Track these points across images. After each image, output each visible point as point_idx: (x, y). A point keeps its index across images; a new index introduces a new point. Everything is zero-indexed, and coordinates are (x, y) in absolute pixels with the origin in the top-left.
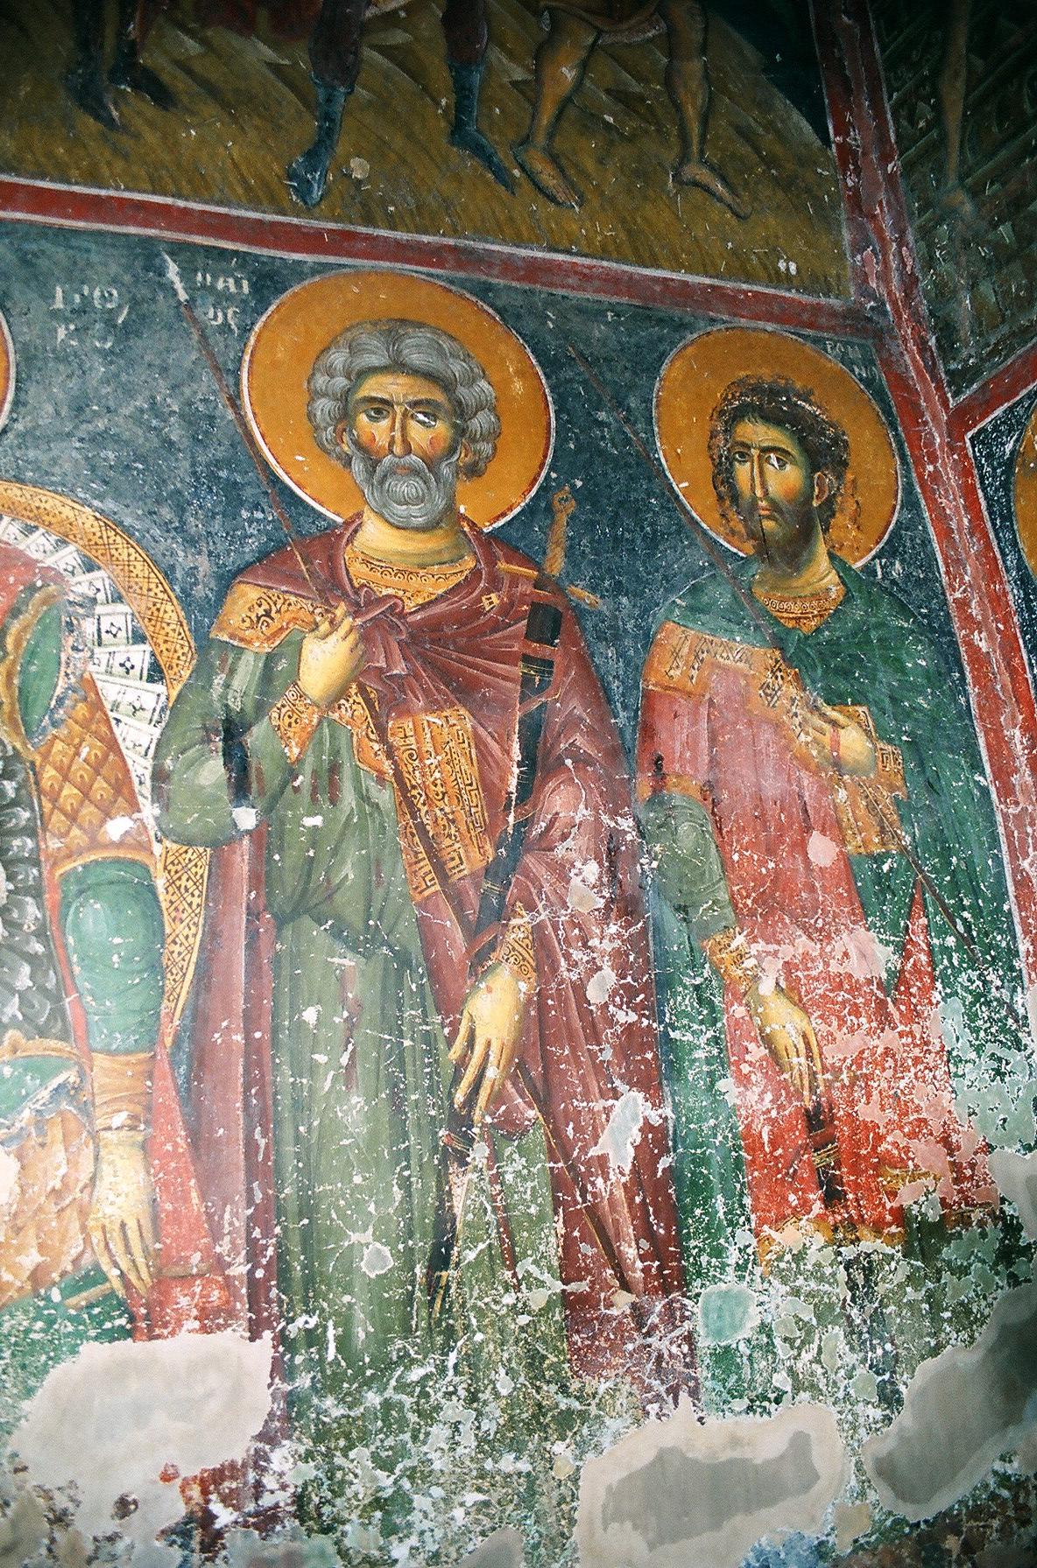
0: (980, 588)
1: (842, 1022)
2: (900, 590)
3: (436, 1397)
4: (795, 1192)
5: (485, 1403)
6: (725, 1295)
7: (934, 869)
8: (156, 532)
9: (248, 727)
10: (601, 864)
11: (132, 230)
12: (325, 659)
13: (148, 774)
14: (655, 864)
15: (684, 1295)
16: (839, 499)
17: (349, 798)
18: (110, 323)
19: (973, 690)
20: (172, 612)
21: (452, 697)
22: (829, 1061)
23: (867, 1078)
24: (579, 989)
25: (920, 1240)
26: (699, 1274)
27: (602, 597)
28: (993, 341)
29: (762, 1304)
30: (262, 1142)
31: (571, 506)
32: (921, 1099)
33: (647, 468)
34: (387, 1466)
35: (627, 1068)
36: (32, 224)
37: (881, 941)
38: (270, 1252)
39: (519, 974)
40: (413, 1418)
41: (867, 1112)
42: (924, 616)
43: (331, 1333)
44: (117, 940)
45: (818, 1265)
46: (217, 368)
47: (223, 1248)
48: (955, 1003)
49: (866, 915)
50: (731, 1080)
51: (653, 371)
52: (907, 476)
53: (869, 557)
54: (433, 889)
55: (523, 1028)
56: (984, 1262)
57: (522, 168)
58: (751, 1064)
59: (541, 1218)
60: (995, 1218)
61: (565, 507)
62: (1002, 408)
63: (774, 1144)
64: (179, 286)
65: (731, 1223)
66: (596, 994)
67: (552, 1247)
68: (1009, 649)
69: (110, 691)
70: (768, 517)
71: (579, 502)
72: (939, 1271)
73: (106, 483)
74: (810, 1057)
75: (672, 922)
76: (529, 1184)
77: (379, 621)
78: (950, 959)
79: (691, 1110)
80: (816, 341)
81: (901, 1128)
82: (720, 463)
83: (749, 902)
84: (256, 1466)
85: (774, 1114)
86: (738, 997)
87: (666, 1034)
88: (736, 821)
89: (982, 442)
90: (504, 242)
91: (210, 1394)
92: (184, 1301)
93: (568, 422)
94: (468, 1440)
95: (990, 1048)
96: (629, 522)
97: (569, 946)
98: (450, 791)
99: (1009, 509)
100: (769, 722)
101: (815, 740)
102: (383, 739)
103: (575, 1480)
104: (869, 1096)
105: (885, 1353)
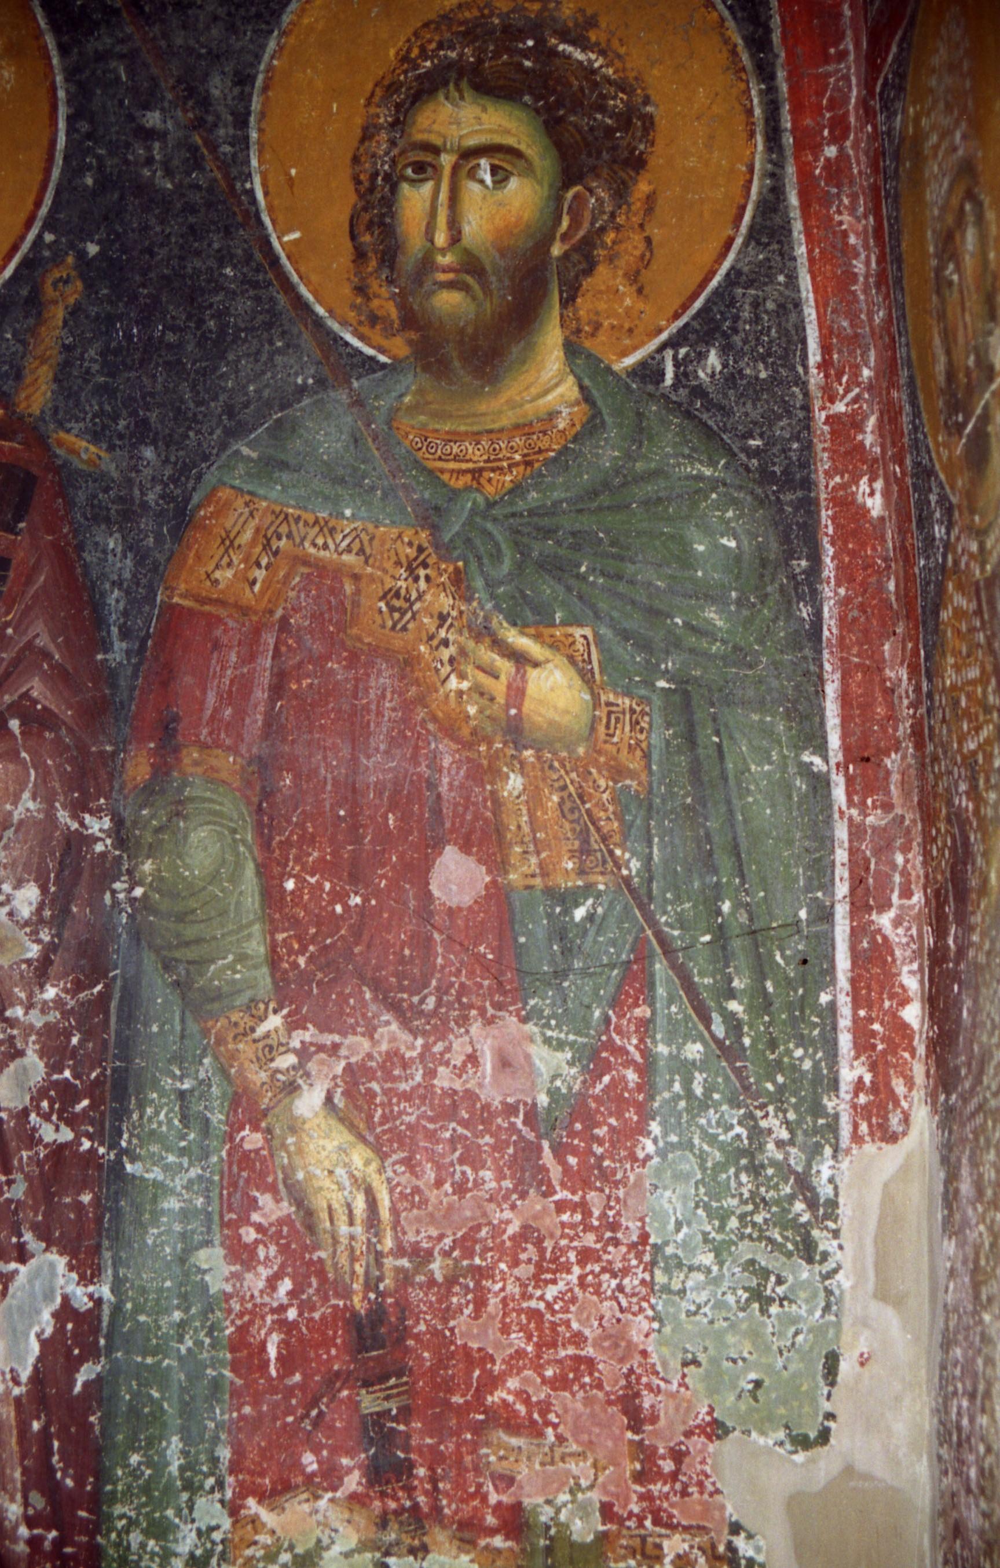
2: (710, 405)
4: (316, 1450)
7: (681, 922)
10: (44, 889)
14: (138, 892)
16: (610, 237)
22: (411, 1237)
23: (481, 1274)
27: (111, 448)
31: (75, 291)
32: (585, 1322)
33: (230, 212)
37: (547, 1041)
42: (757, 453)
49: (520, 994)
50: (219, 1252)
58: (259, 1228)
61: (64, 294)
65: (189, 1486)
70: (451, 285)
71: (90, 286)
78: (687, 1083)
81: (539, 1369)
82: (371, 190)
83: (302, 961)
87: (119, 1164)
88: (301, 825)
93: (89, 136)
95: (745, 1250)
96: (177, 313)
104: (480, 1303)
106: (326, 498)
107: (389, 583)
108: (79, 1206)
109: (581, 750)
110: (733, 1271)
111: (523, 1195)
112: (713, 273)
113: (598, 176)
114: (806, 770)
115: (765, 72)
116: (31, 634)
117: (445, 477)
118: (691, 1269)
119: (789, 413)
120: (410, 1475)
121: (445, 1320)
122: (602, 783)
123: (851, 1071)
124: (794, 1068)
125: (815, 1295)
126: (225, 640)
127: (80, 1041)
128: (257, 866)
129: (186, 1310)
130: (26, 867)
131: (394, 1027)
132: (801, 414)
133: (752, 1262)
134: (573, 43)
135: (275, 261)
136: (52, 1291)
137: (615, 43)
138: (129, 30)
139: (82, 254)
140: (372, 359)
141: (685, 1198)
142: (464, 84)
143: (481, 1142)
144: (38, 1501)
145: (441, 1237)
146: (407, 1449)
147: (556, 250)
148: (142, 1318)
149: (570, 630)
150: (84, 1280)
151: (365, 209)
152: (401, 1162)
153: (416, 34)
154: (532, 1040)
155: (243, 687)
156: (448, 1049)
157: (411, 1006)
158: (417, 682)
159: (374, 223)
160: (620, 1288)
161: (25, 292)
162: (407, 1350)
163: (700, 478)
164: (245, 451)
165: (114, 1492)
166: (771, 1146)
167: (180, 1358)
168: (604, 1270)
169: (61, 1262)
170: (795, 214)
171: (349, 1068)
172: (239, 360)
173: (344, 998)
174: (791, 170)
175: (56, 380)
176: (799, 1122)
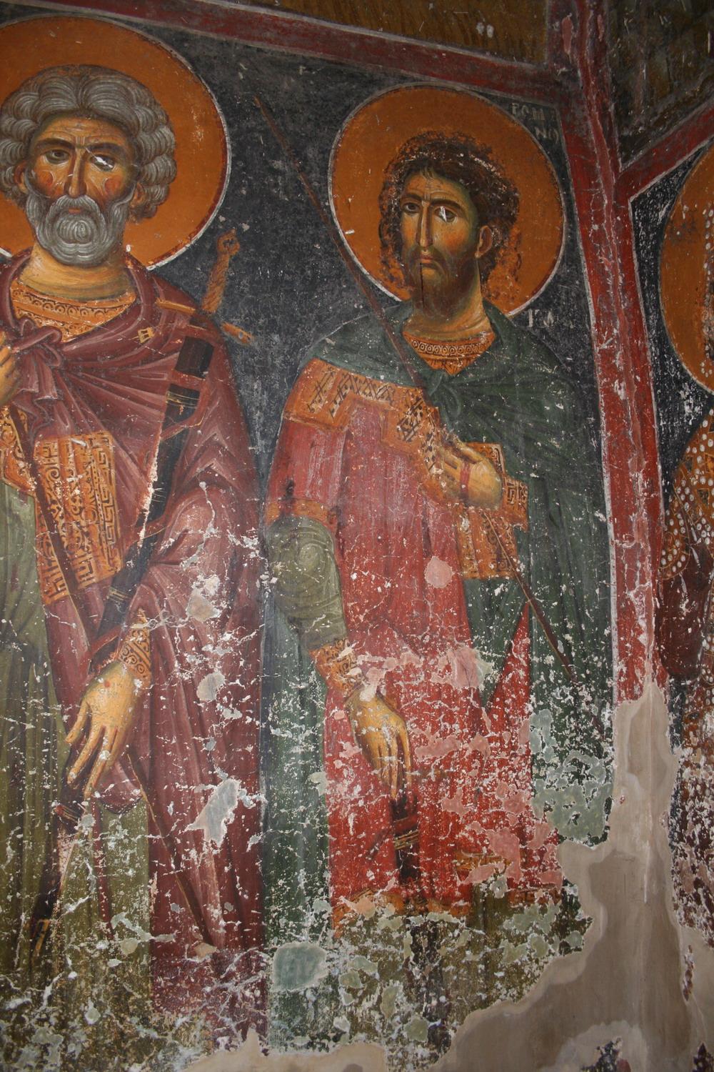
0: (625, 342)
1: (436, 726)
2: (549, 339)
4: (374, 869)
5: (73, 1030)
7: (544, 595)
10: (222, 579)
14: (274, 580)
15: (261, 950)
16: (502, 252)
19: (605, 434)
21: (98, 422)
22: (420, 760)
24: (190, 688)
25: (484, 913)
26: (277, 933)
27: (255, 334)
28: (660, 110)
29: (331, 960)
31: (236, 249)
35: (228, 758)
37: (483, 657)
39: (133, 674)
41: (446, 804)
42: (569, 364)
45: (387, 930)
48: (546, 714)
49: (472, 634)
51: (335, 123)
52: (572, 233)
53: (523, 307)
54: (63, 594)
56: (540, 932)
58: (344, 760)
59: (138, 879)
60: (556, 897)
61: (230, 250)
62: (661, 176)
63: (358, 828)
66: (204, 693)
67: (145, 904)
68: (642, 399)
70: (429, 266)
71: (244, 246)
72: (498, 939)
74: (401, 755)
75: (286, 634)
76: (129, 852)
78: (547, 676)
79: (284, 797)
80: (503, 102)
81: (480, 819)
83: (361, 617)
86: (340, 703)
87: (267, 731)
88: (359, 544)
89: (641, 208)
93: (244, 169)
95: (573, 754)
97: (184, 650)
98: (88, 506)
99: (656, 272)
100: (402, 454)
101: (446, 474)
102: (28, 457)
104: (453, 790)
105: (439, 1004)
106: (371, 369)
107: (402, 416)
108: (245, 753)
109: (496, 508)
110: (567, 764)
111: (473, 735)
112: (548, 276)
113: (495, 223)
114: (597, 519)
115: (565, 186)
116: (211, 434)
117: (429, 362)
118: (549, 765)
119: (584, 347)
120: (420, 877)
121: (436, 800)
122: (506, 524)
123: (618, 666)
124: (594, 666)
125: (602, 773)
126: (317, 442)
127: (245, 664)
128: (337, 566)
129: (306, 805)
130: (211, 565)
131: (410, 652)
132: (588, 347)
133: (575, 760)
134: (481, 158)
135: (341, 243)
136: (233, 798)
137: (500, 162)
138: (265, 119)
139: (240, 230)
140: (392, 298)
141: (546, 732)
142: (431, 169)
143: (453, 710)
144: (229, 907)
145: (434, 760)
146: (418, 864)
147: (477, 255)
148: (283, 811)
149: (490, 445)
150: (250, 792)
151: (386, 223)
152: (415, 722)
153: (408, 142)
154: (476, 657)
155: (328, 467)
156: (436, 663)
157: (418, 641)
158: (416, 469)
159: (390, 228)
160: (517, 777)
161: (208, 246)
162: (418, 816)
163: (546, 373)
164: (329, 341)
165: (270, 900)
166: (584, 704)
167: (304, 830)
168: (510, 769)
169: (237, 783)
170: (582, 253)
171: (389, 675)
172: (323, 292)
173: (385, 637)
174: (579, 233)
175: (224, 295)
176: (597, 691)
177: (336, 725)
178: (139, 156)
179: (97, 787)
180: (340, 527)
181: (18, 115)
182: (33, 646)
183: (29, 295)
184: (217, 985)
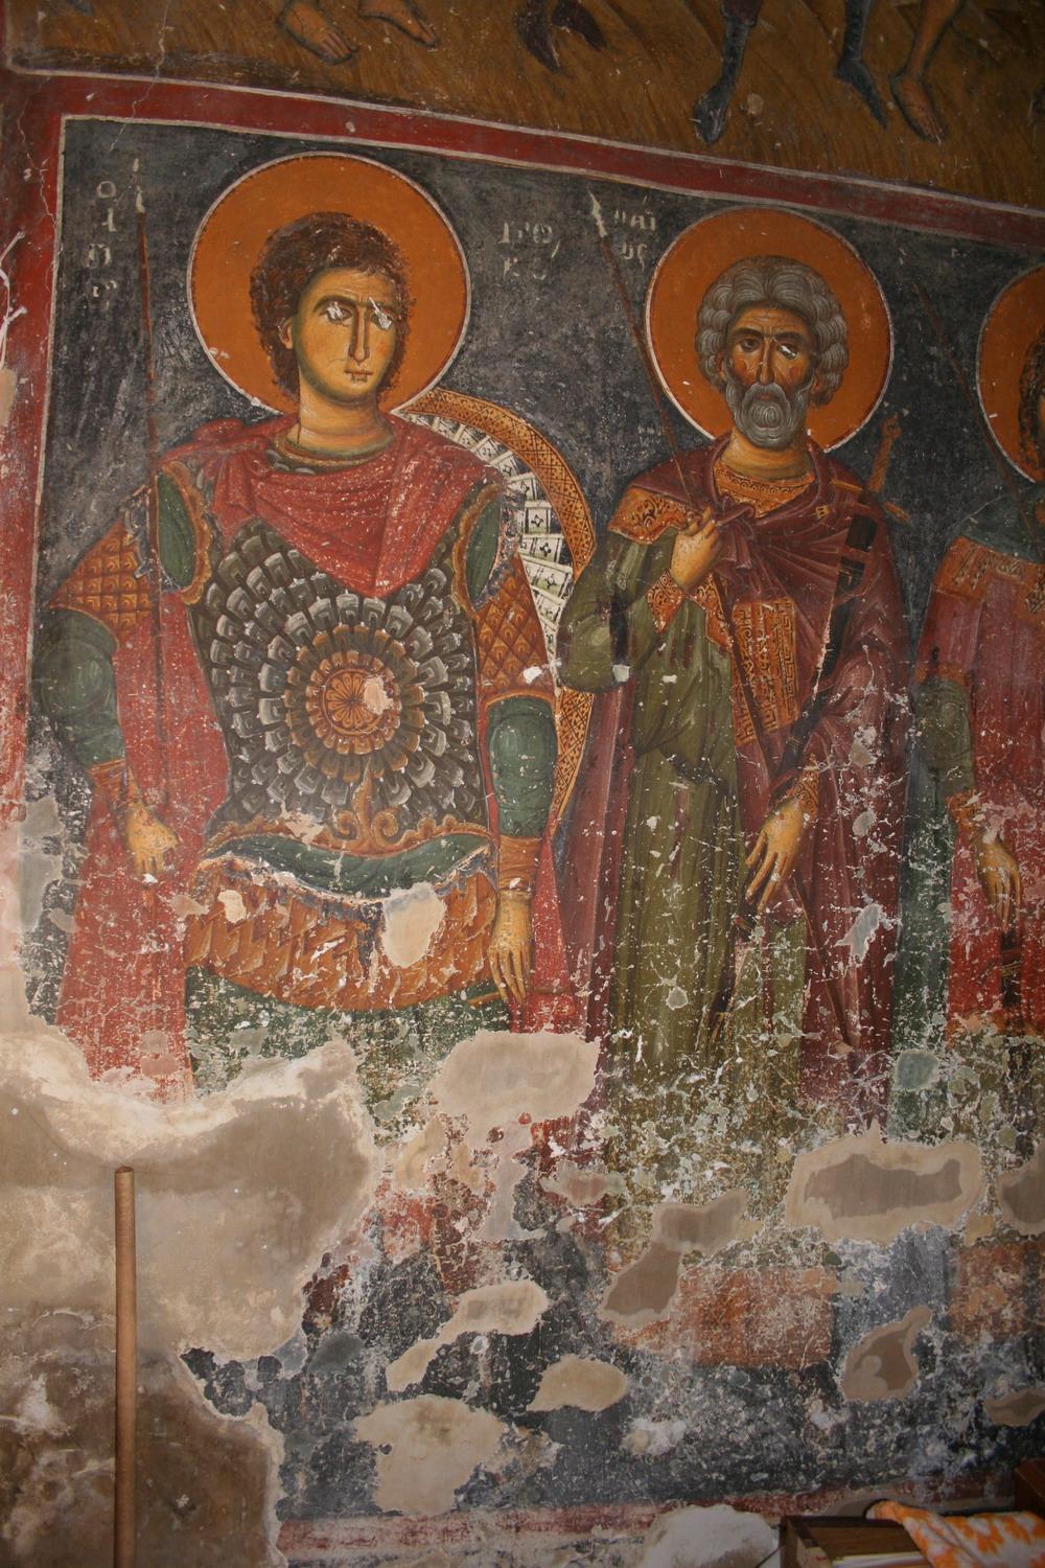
3: (705, 1096)
4: (983, 992)
6: (918, 1057)
8: (573, 442)
9: (629, 604)
10: (878, 730)
11: (565, 169)
12: (690, 551)
13: (555, 634)
17: (698, 663)
18: (545, 257)
20: (580, 509)
26: (901, 1040)
27: (911, 512)
30: (609, 908)
33: (965, 400)
34: (666, 1136)
36: (486, 163)
38: (606, 984)
39: (804, 808)
40: (687, 1107)
43: (640, 1044)
44: (524, 757)
45: (990, 1047)
46: (627, 301)
47: (575, 978)
50: (949, 904)
51: (983, 307)
55: (802, 847)
57: (897, 100)
59: (795, 984)
61: (892, 433)
63: (973, 955)
64: (600, 223)
66: (858, 829)
67: (799, 1006)
69: (532, 569)
73: (537, 398)
74: (1013, 894)
75: (926, 782)
77: (735, 525)
84: (581, 1123)
85: (977, 933)
86: (966, 844)
90: (871, 177)
91: (557, 1073)
92: (545, 1010)
94: (721, 1129)
97: (845, 790)
102: (728, 620)
103: (790, 1164)
105: (1028, 1116)
108: (888, 882)
135: (986, 427)
139: (901, 414)
144: (866, 1013)
150: (890, 916)
171: (1008, 822)
177: (961, 862)
178: (817, 344)
179: (768, 904)
180: (974, 689)
181: (716, 306)
182: (726, 781)
183: (729, 474)
184: (850, 1079)
